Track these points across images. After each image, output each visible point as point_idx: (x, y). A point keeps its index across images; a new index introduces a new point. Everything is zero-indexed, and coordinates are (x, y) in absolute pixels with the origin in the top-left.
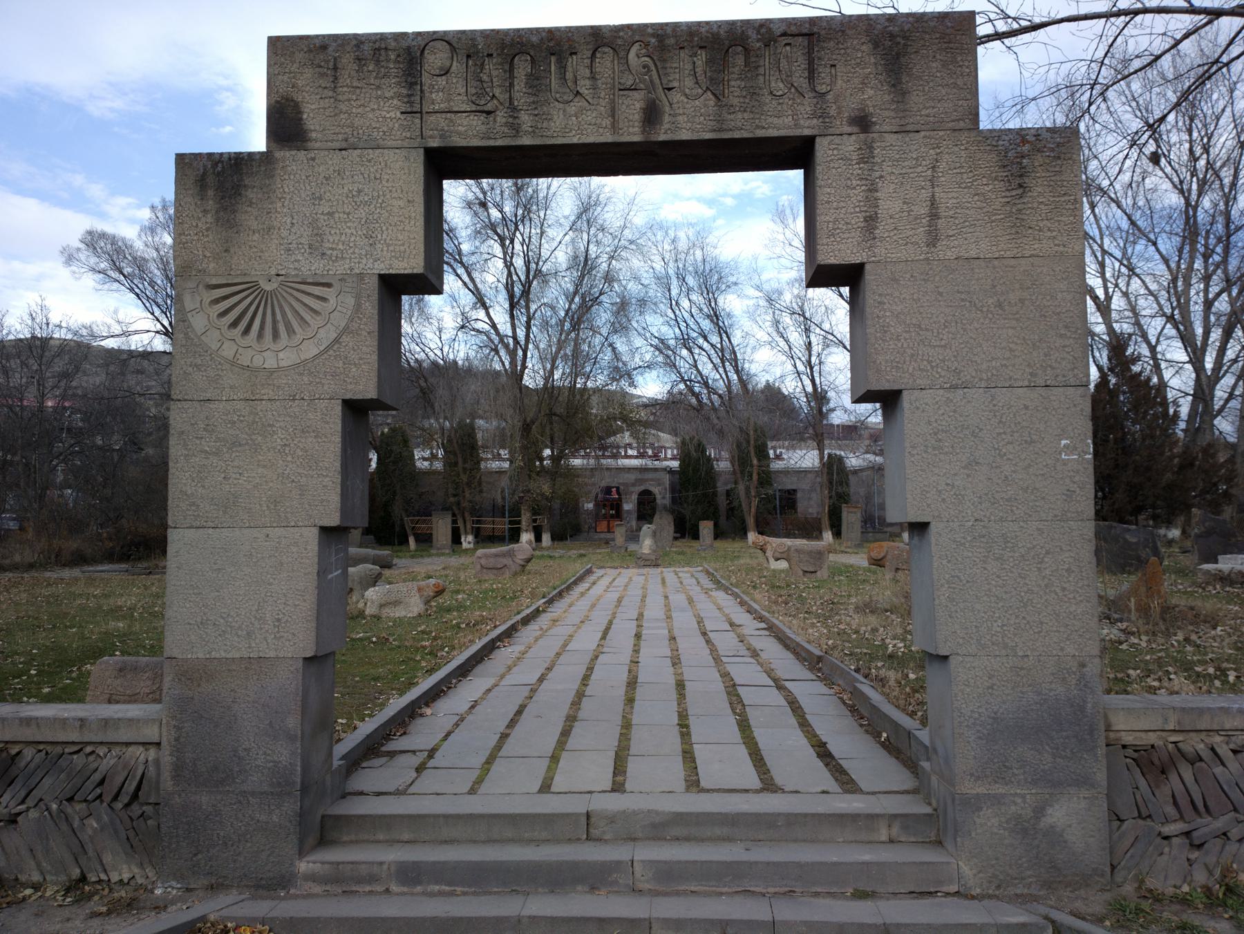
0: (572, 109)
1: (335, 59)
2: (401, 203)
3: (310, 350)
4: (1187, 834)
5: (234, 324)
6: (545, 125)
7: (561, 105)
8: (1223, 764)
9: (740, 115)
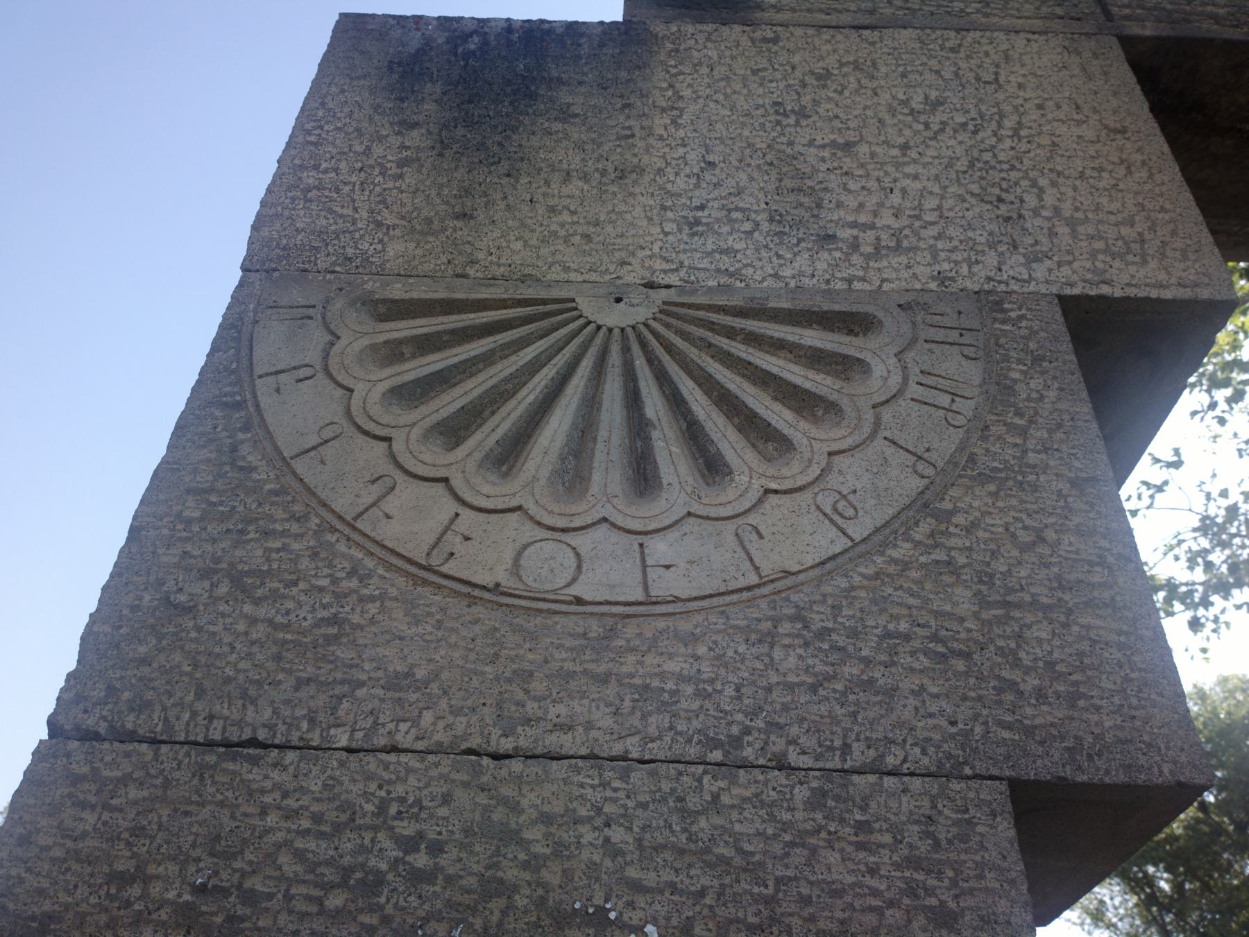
3: (798, 538)
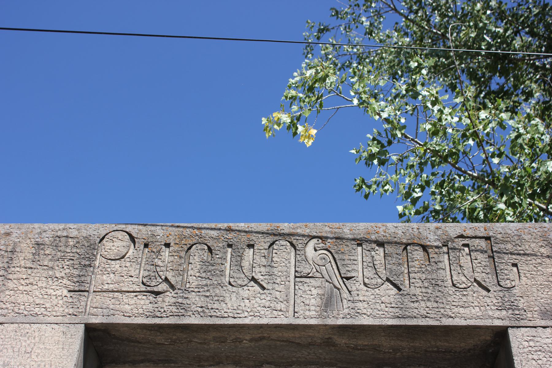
0: (245, 293)
1: (15, 243)
6: (215, 306)
7: (234, 289)
9: (423, 304)
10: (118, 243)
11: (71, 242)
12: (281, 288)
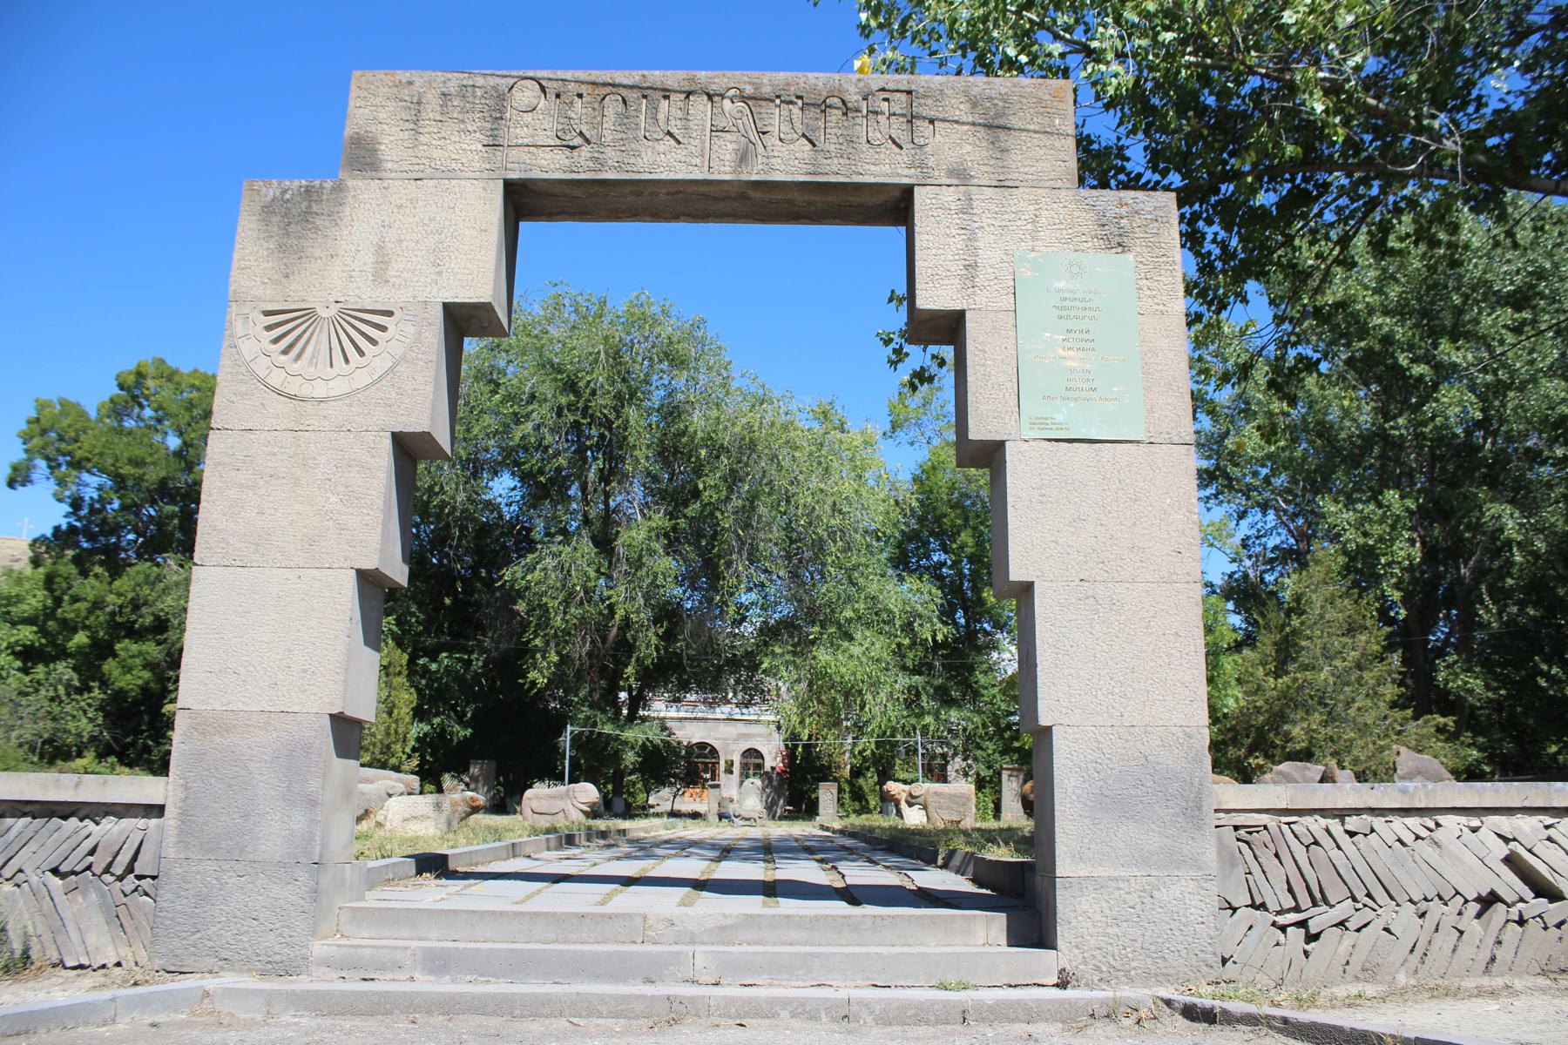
0: (661, 147)
2: (474, 233)
3: (363, 379)
4: (1302, 924)
5: (285, 352)
8: (1339, 848)
10: (528, 93)
11: (479, 92)
12: (697, 142)
